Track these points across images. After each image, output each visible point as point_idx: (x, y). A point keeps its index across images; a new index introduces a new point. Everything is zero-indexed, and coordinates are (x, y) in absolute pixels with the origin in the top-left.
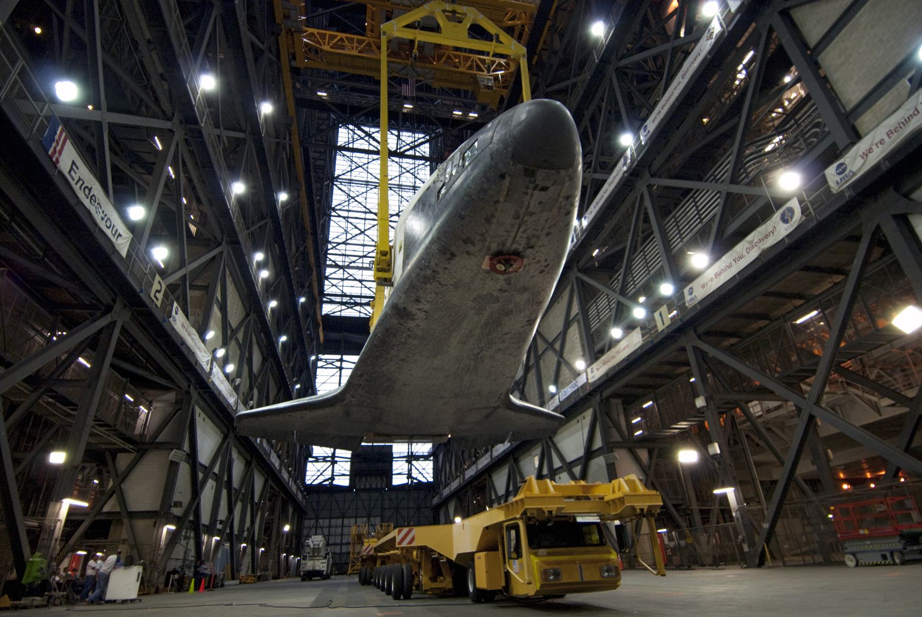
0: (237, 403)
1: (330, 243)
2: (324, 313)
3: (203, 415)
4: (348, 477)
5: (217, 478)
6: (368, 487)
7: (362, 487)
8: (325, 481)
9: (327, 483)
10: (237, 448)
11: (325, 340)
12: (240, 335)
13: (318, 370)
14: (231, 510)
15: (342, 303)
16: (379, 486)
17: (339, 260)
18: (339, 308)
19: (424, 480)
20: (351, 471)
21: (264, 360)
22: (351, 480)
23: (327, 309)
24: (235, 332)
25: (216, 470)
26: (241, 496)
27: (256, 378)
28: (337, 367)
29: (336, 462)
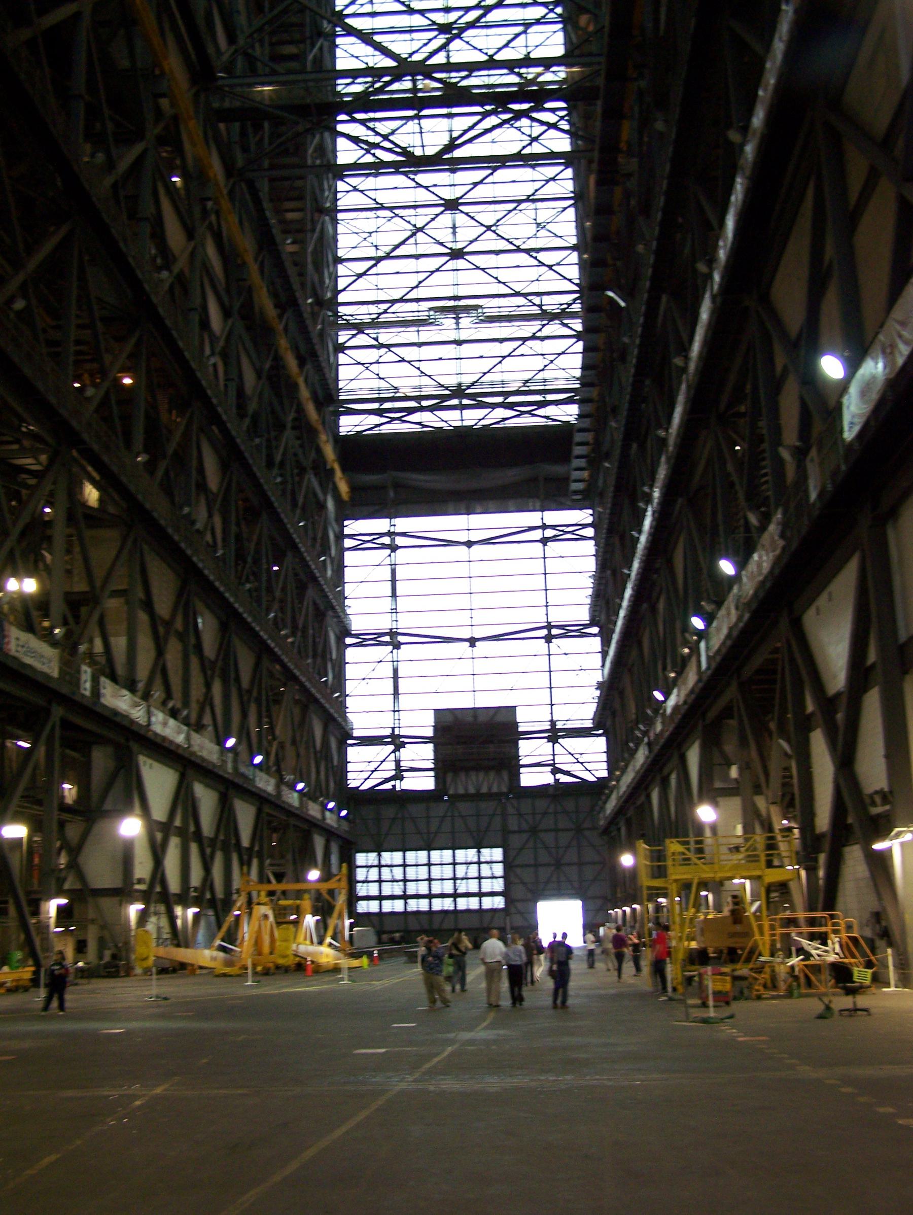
0: (188, 738)
1: (341, 261)
2: (343, 431)
3: (149, 761)
4: (432, 773)
5: (182, 832)
6: (472, 790)
7: (461, 791)
8: (387, 780)
9: (388, 786)
10: (200, 782)
11: (353, 489)
12: (179, 624)
13: (347, 554)
14: (207, 868)
15: (379, 412)
16: (495, 789)
17: (363, 313)
18: (375, 420)
19: (591, 778)
20: (436, 760)
21: (224, 628)
22: (436, 777)
23: (348, 425)
24: (168, 624)
25: (178, 822)
26: (219, 844)
27: (213, 663)
28: (384, 546)
29: (403, 745)
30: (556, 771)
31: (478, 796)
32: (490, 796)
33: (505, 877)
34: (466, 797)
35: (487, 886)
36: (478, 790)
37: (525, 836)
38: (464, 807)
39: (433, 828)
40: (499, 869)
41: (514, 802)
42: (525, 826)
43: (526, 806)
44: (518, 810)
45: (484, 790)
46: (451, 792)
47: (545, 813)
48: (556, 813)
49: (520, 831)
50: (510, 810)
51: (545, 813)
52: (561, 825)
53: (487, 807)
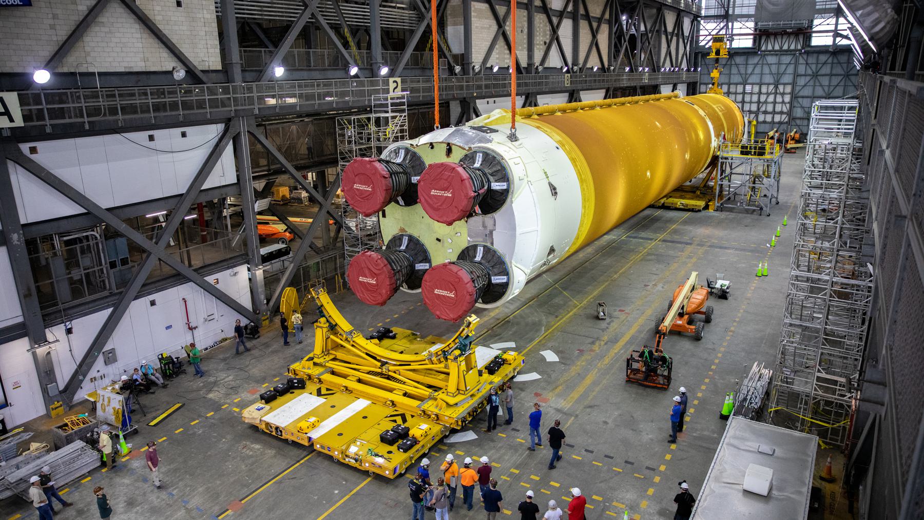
6: (777, 47)
7: (770, 48)
30: (836, 34)
31: (781, 52)
32: (788, 52)
33: (791, 103)
34: (774, 52)
35: (778, 108)
36: (781, 48)
37: (808, 78)
38: (771, 59)
39: (749, 71)
40: (787, 98)
41: (805, 56)
42: (809, 72)
43: (812, 60)
44: (806, 61)
45: (785, 47)
46: (763, 48)
47: (825, 63)
48: (833, 63)
49: (805, 75)
50: (801, 61)
51: (825, 63)
52: (834, 72)
53: (786, 59)
